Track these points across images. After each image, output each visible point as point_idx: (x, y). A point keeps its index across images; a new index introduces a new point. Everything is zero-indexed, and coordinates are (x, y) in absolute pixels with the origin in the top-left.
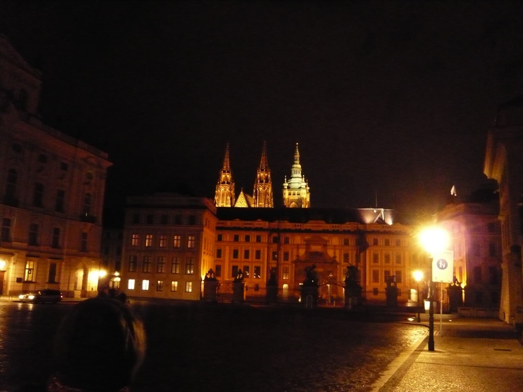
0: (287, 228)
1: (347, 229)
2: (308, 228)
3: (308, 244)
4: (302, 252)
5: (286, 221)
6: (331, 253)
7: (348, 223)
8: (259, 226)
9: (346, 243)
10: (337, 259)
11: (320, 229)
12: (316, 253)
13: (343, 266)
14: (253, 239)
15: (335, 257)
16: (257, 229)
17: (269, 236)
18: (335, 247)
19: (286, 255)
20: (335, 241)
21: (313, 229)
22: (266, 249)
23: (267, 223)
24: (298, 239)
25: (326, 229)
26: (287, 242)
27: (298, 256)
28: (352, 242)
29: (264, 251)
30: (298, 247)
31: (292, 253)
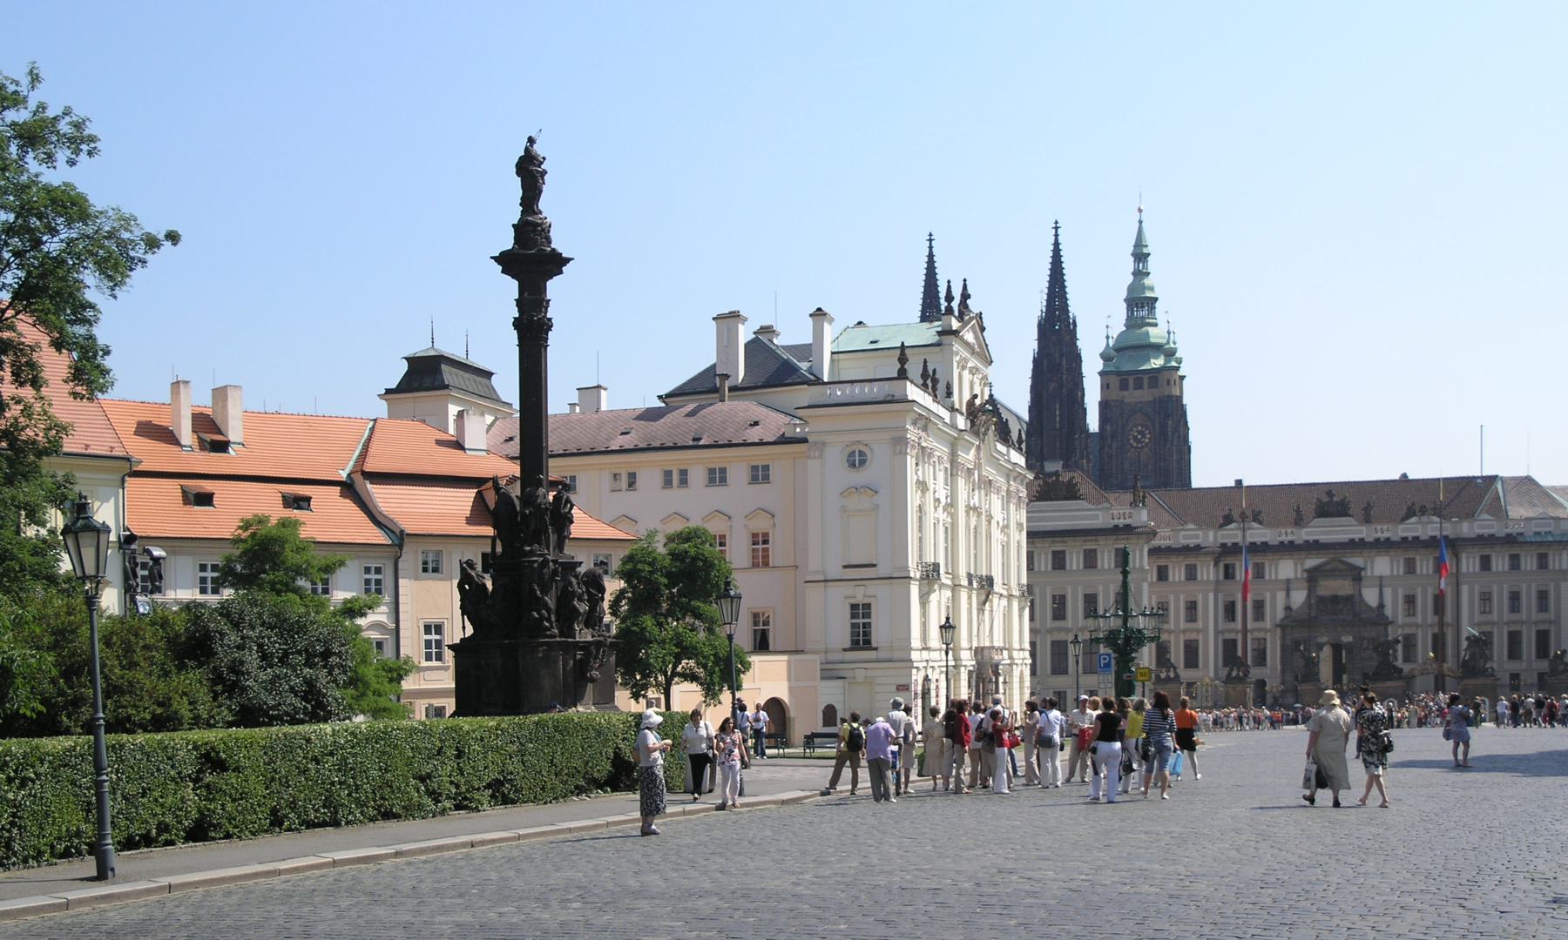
0: (1258, 540)
1: (1410, 535)
2: (1311, 538)
3: (1313, 576)
4: (1299, 597)
5: (1255, 525)
6: (1370, 596)
7: (1414, 519)
8: (1192, 542)
9: (1410, 567)
10: (1388, 612)
11: (1344, 538)
12: (1335, 599)
13: (1403, 626)
14: (1177, 573)
15: (1381, 606)
16: (1186, 550)
17: (1216, 565)
18: (1381, 582)
19: (1259, 606)
20: (1382, 566)
21: (1323, 538)
22: (1211, 595)
23: (1211, 534)
24: (1286, 569)
25: (1357, 537)
26: (1259, 574)
27: (1288, 608)
28: (1425, 565)
29: (1206, 599)
30: (1288, 586)
31: (1274, 597)
